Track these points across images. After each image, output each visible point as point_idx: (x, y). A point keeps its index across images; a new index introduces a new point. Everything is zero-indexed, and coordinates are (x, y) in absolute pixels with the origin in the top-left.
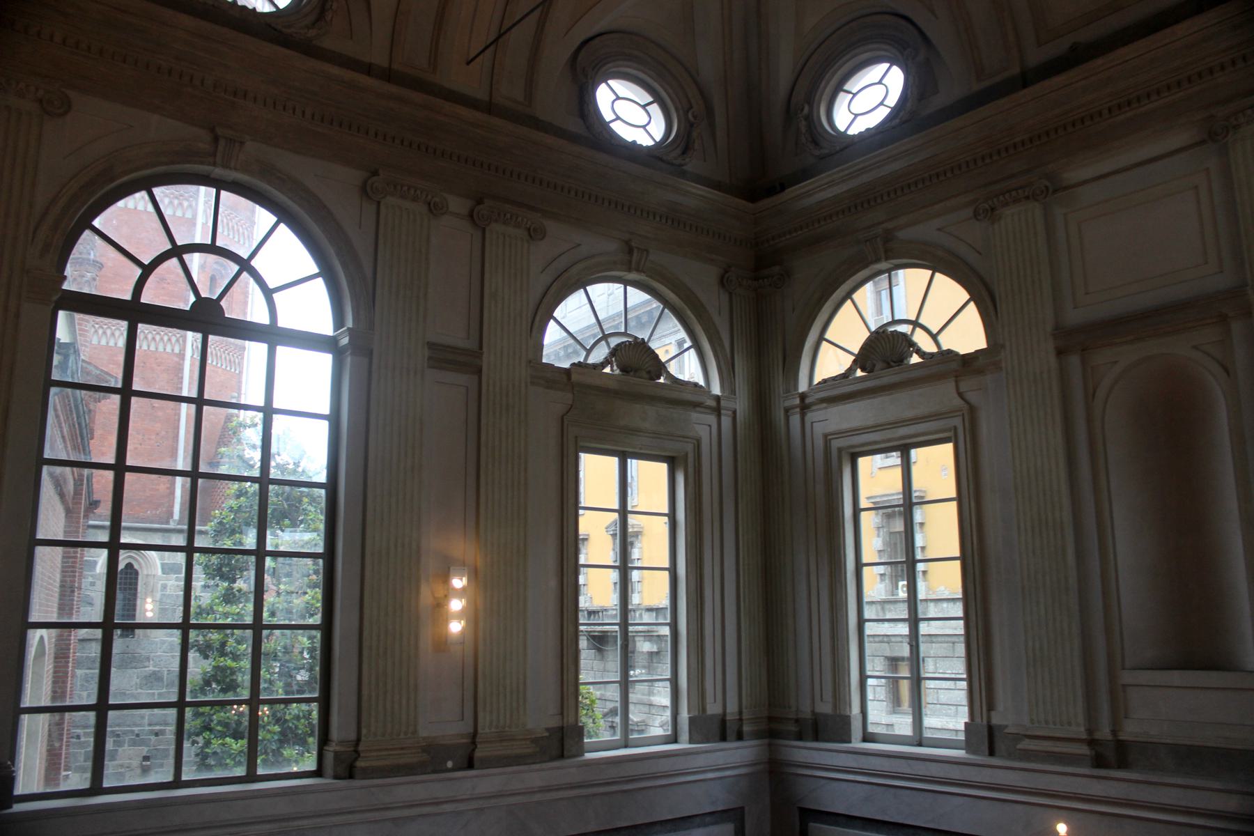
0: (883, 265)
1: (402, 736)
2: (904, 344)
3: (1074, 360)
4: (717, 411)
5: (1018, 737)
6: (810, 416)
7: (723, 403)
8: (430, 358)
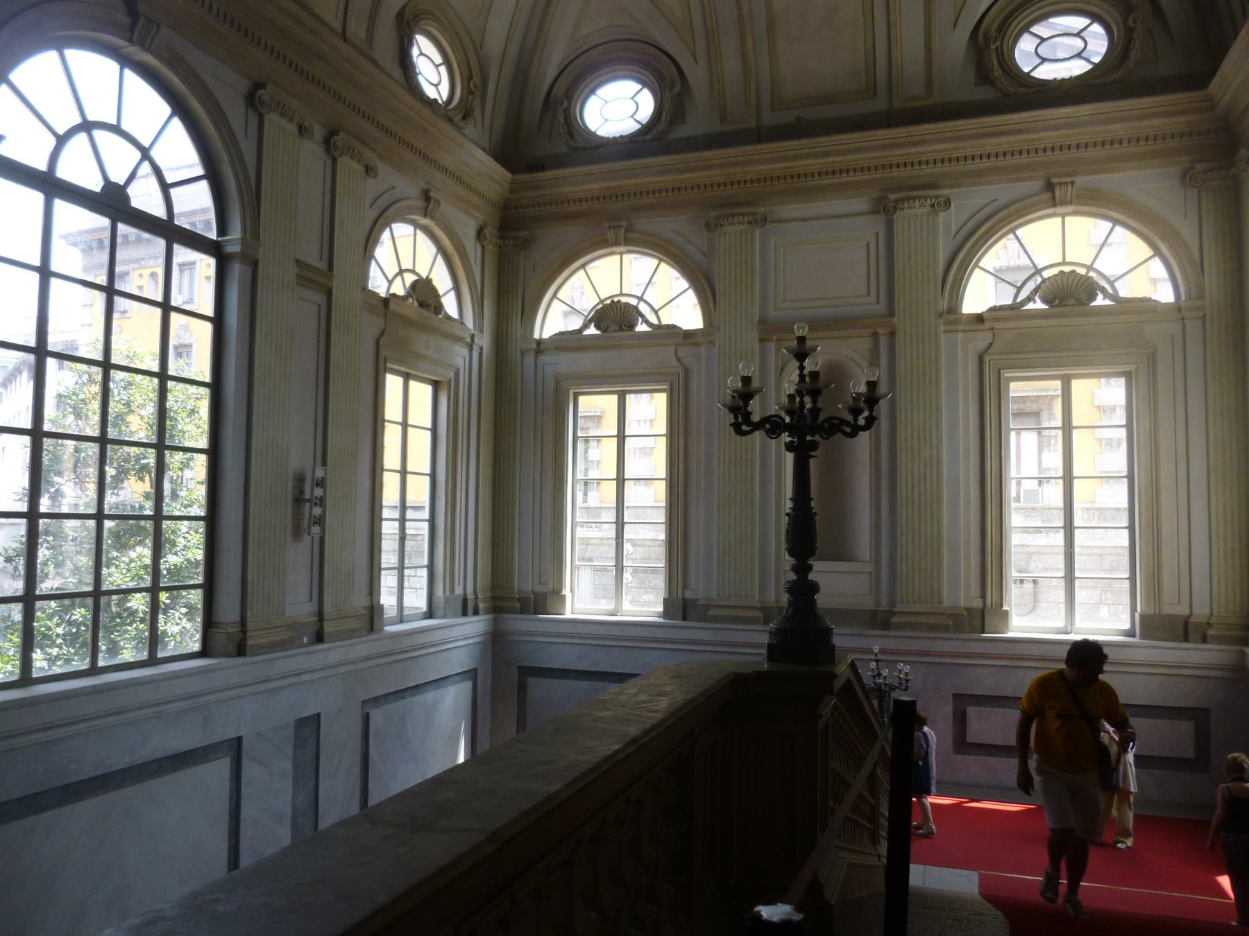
0: (622, 249)
1: (274, 617)
2: (634, 313)
3: (772, 346)
4: (471, 347)
5: (709, 607)
6: (542, 358)
7: (476, 339)
8: (298, 275)
